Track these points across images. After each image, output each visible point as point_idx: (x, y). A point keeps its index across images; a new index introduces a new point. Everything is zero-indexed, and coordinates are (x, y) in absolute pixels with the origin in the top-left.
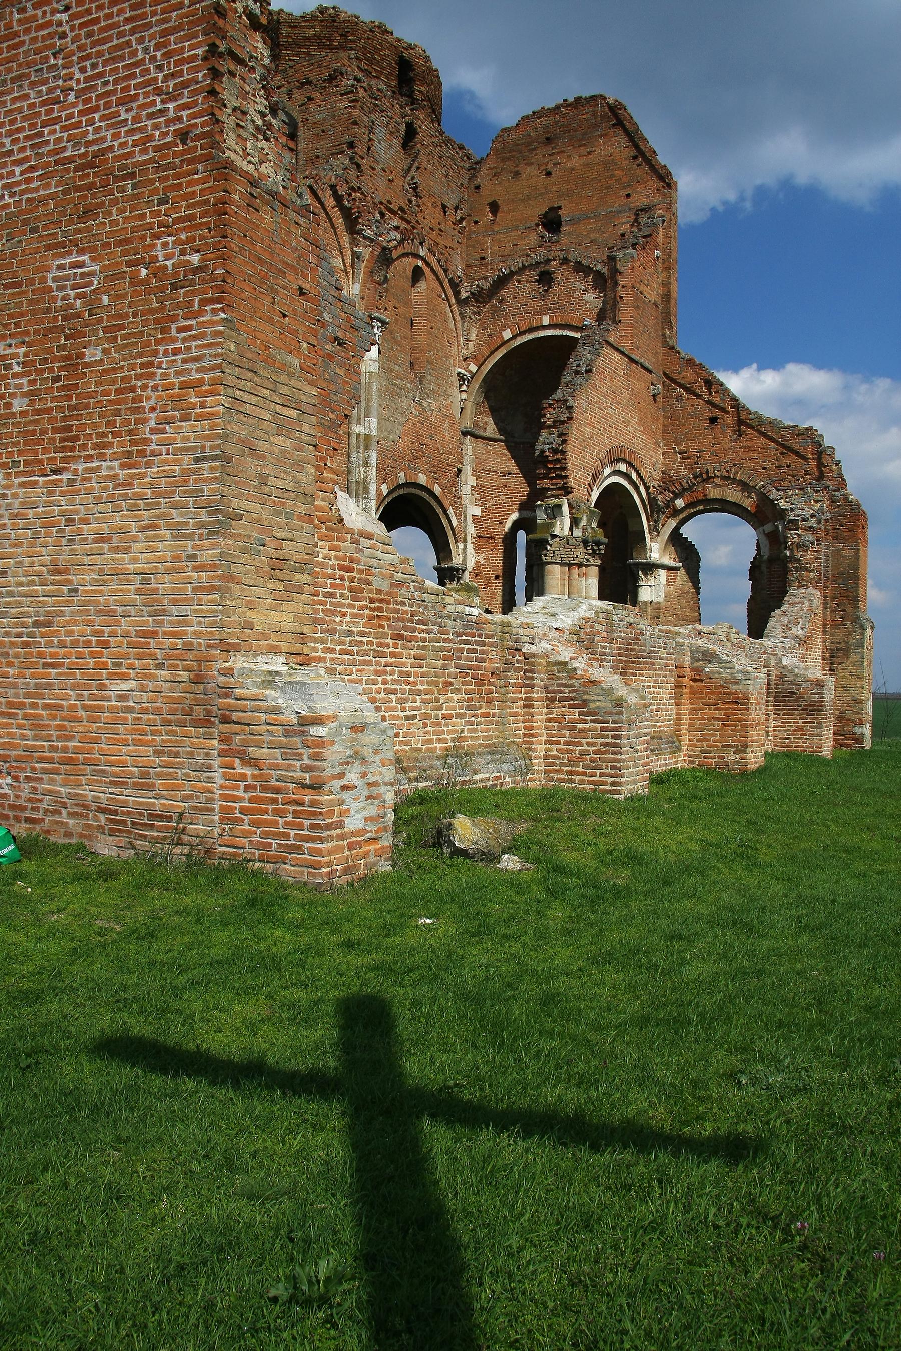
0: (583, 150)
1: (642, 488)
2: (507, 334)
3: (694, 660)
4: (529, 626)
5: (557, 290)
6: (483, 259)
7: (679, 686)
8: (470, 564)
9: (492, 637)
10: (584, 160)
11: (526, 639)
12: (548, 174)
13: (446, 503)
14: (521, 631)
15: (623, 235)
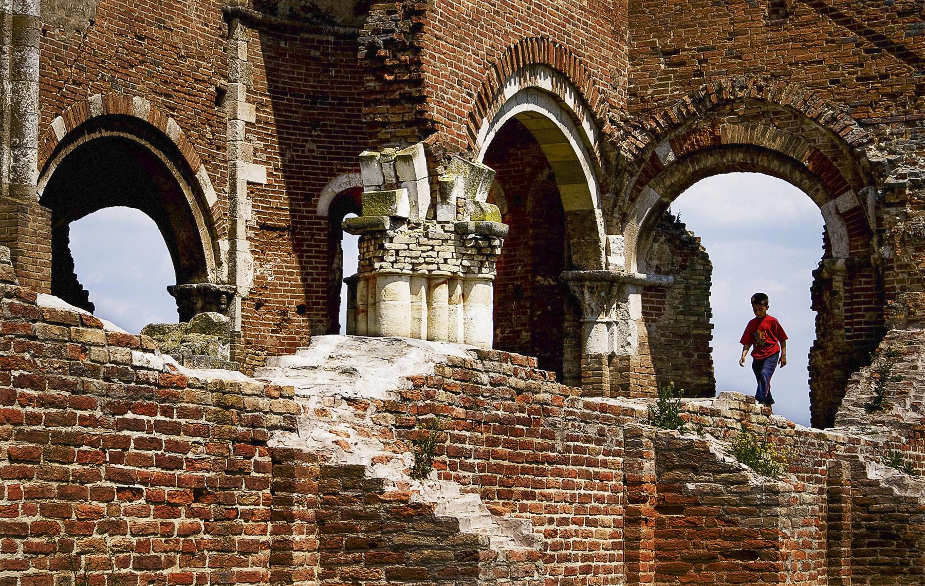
1: (586, 125)
3: (663, 464)
4: (282, 393)
7: (632, 519)
8: (245, 282)
9: (197, 414)
11: (275, 419)
13: (191, 157)
14: (264, 403)
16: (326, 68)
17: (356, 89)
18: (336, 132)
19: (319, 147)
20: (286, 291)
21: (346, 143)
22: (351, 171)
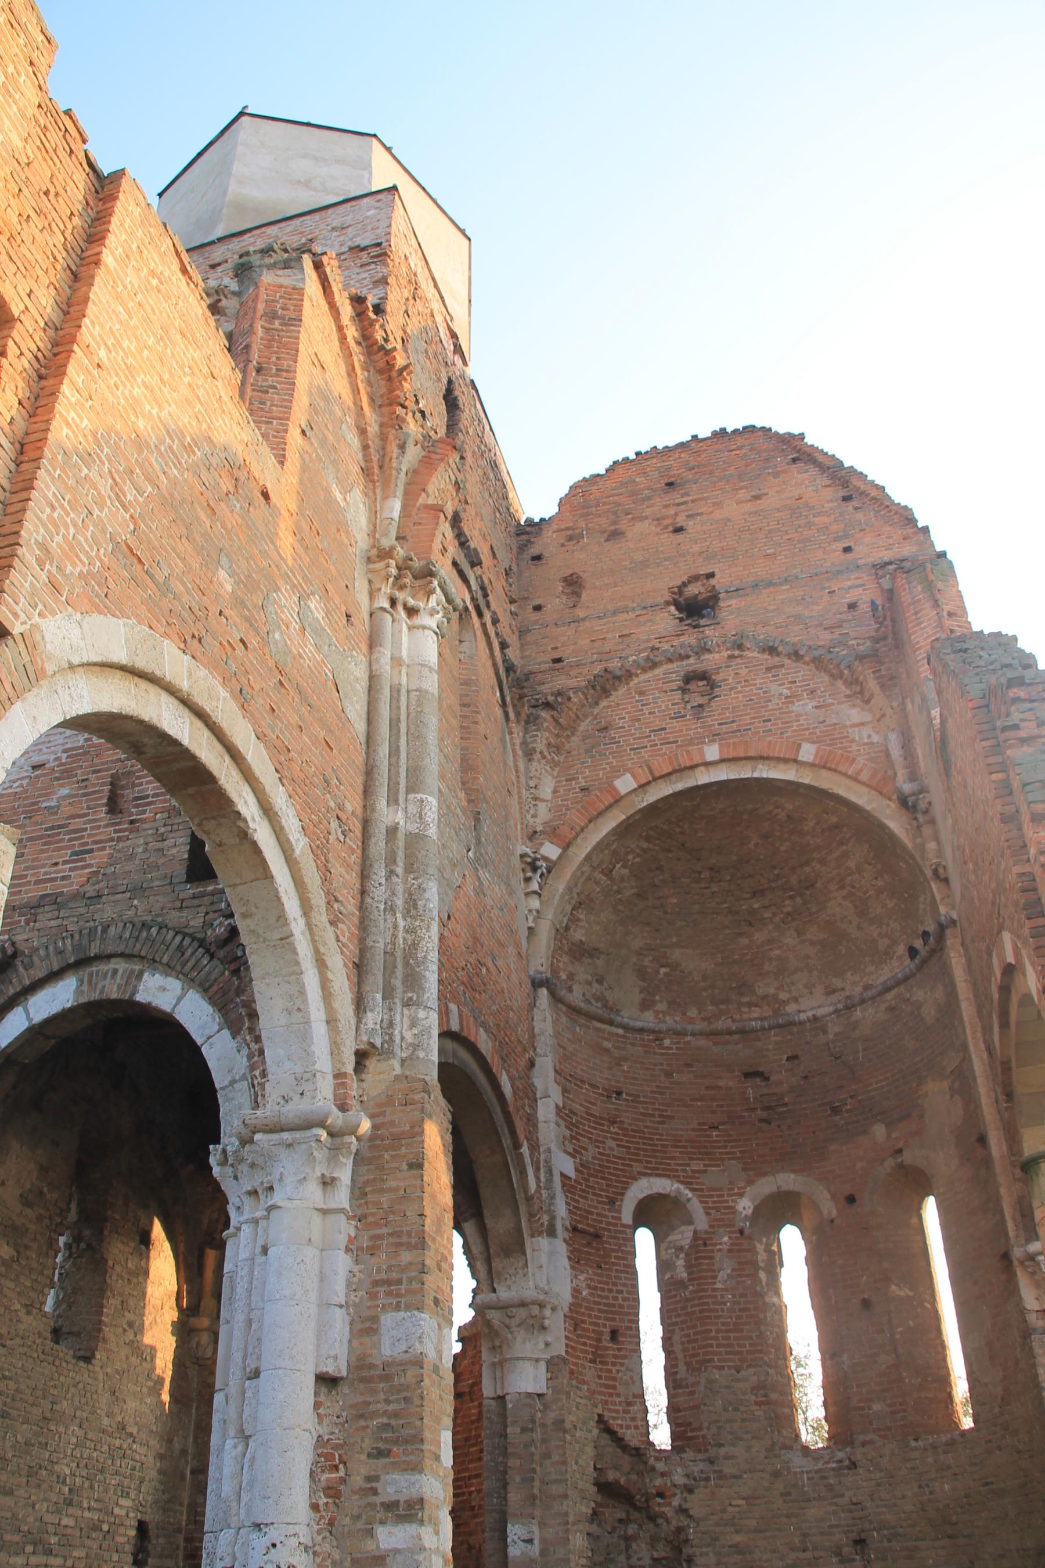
0: (742, 494)
2: (625, 784)
5: (730, 700)
6: (558, 660)
10: (748, 507)
12: (679, 530)
15: (852, 606)
16: (618, 1062)
17: (648, 1086)
18: (633, 1131)
19: (618, 1146)
20: (600, 1311)
21: (644, 1144)
22: (650, 1175)
